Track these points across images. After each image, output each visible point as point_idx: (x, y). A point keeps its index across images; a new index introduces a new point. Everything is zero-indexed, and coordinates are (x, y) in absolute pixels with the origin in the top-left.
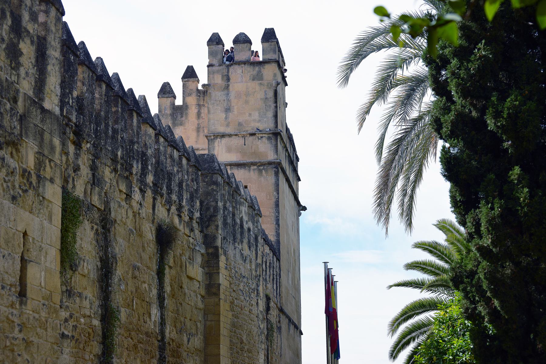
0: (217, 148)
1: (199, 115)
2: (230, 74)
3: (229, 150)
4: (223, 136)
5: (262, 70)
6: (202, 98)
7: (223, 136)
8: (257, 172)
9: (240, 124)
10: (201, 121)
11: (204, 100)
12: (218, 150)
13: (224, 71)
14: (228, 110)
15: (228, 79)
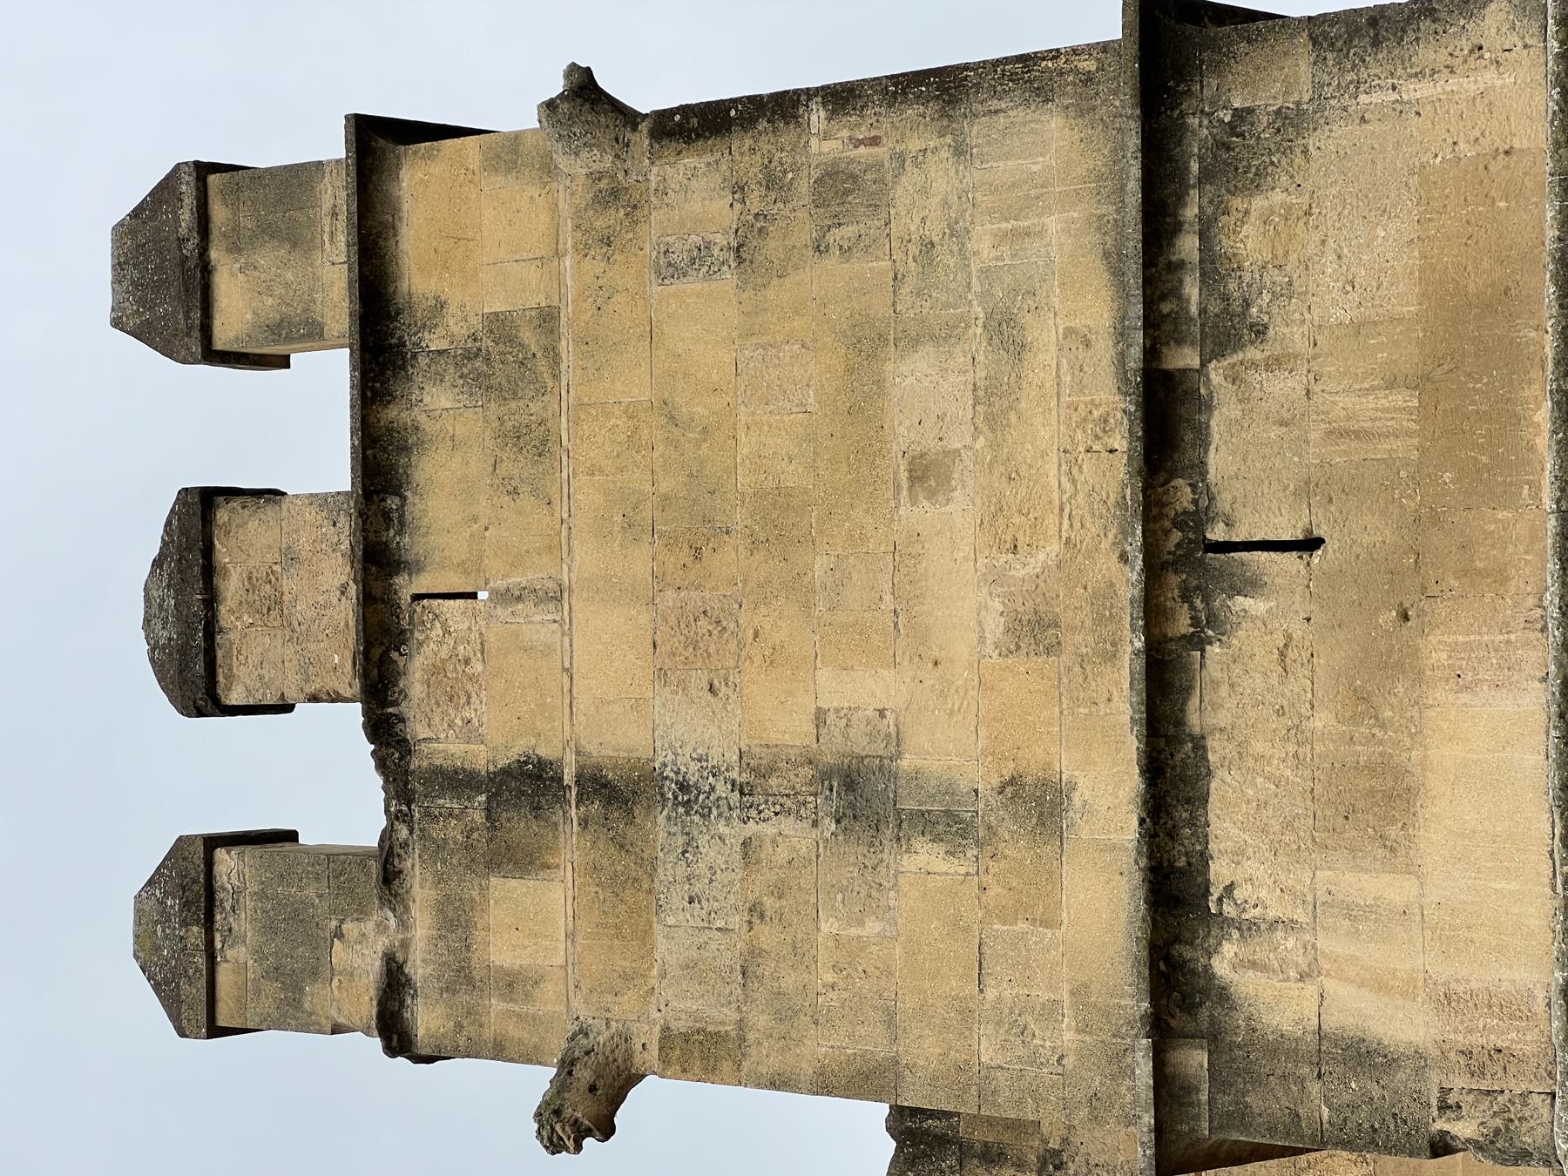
2: (480, 757)
3: (1374, 803)
4: (1174, 895)
7: (1174, 895)
9: (1034, 630)
12: (1381, 986)
13: (453, 831)
14: (861, 796)
15: (529, 784)
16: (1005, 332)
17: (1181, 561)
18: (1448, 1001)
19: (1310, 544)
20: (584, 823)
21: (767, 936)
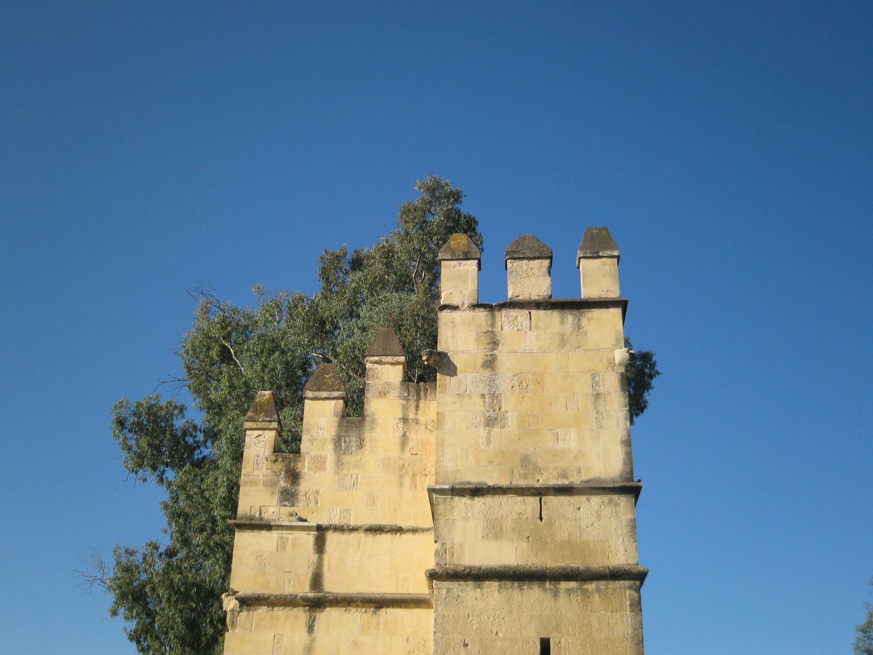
2: (498, 329)
3: (495, 531)
6: (412, 404)
8: (576, 600)
9: (526, 461)
17: (540, 492)
19: (541, 519)
20: (486, 355)
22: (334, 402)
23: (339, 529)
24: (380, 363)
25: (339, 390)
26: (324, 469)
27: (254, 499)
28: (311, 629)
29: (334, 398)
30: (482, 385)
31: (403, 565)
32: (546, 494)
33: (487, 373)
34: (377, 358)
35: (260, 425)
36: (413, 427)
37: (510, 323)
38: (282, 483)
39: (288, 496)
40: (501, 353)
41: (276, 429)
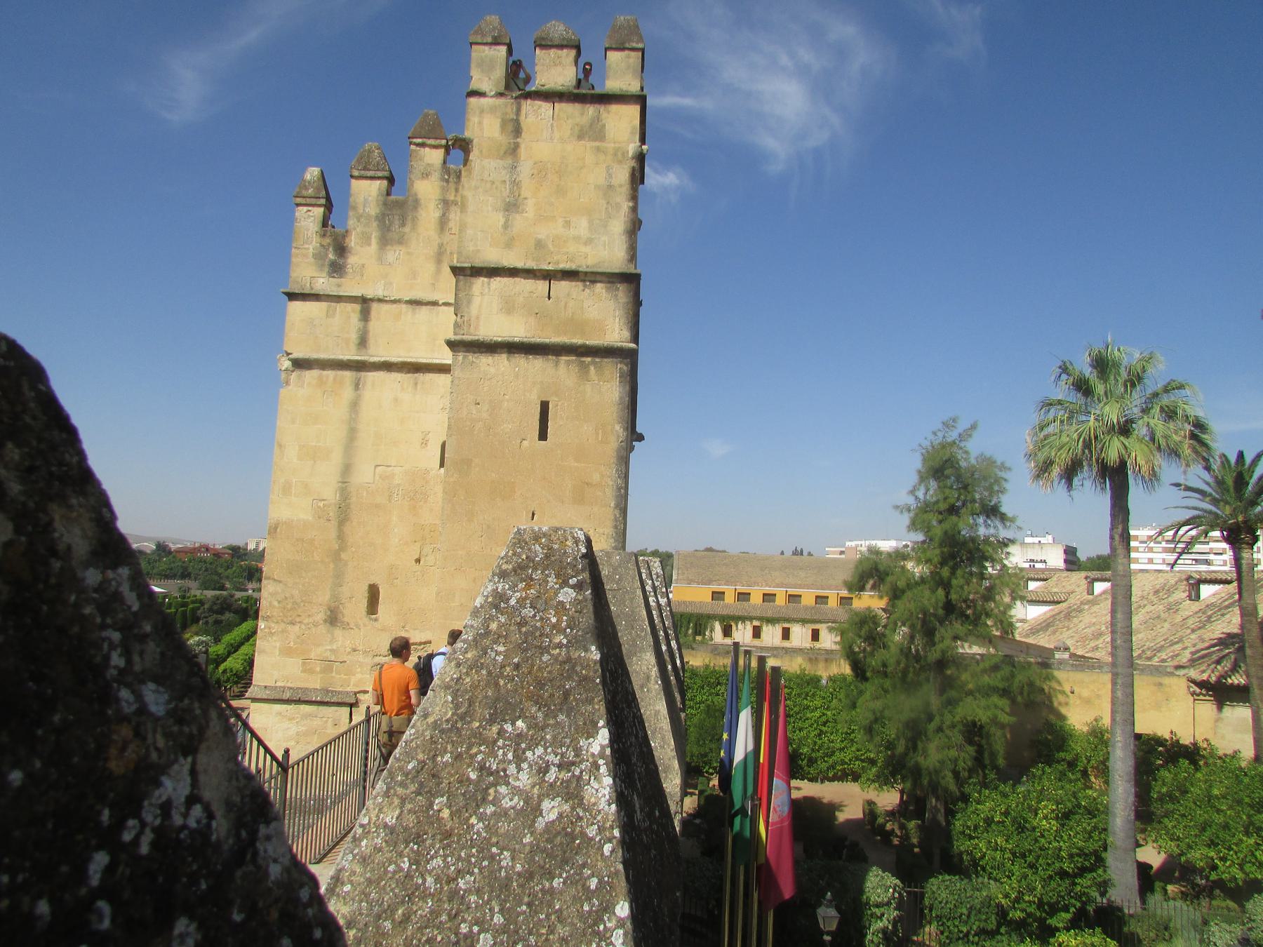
0: (476, 301)
1: (443, 223)
2: (522, 118)
3: (509, 307)
4: (493, 272)
5: (604, 115)
6: (452, 186)
7: (493, 272)
8: (574, 368)
9: (539, 245)
10: (447, 237)
11: (457, 190)
12: (480, 306)
13: (509, 110)
14: (512, 207)
15: (518, 131)
16: (589, 242)
17: (548, 276)
18: (478, 318)
21: (489, 185)
22: (378, 182)
23: (380, 300)
24: (423, 145)
25: (383, 170)
26: (370, 245)
27: (306, 270)
28: (357, 386)
29: (379, 178)
30: (504, 172)
31: (425, 337)
32: (556, 279)
33: (509, 161)
34: (419, 141)
35: (309, 201)
36: (453, 208)
37: (537, 114)
38: (331, 256)
39: (337, 269)
40: (524, 141)
41: (325, 206)
